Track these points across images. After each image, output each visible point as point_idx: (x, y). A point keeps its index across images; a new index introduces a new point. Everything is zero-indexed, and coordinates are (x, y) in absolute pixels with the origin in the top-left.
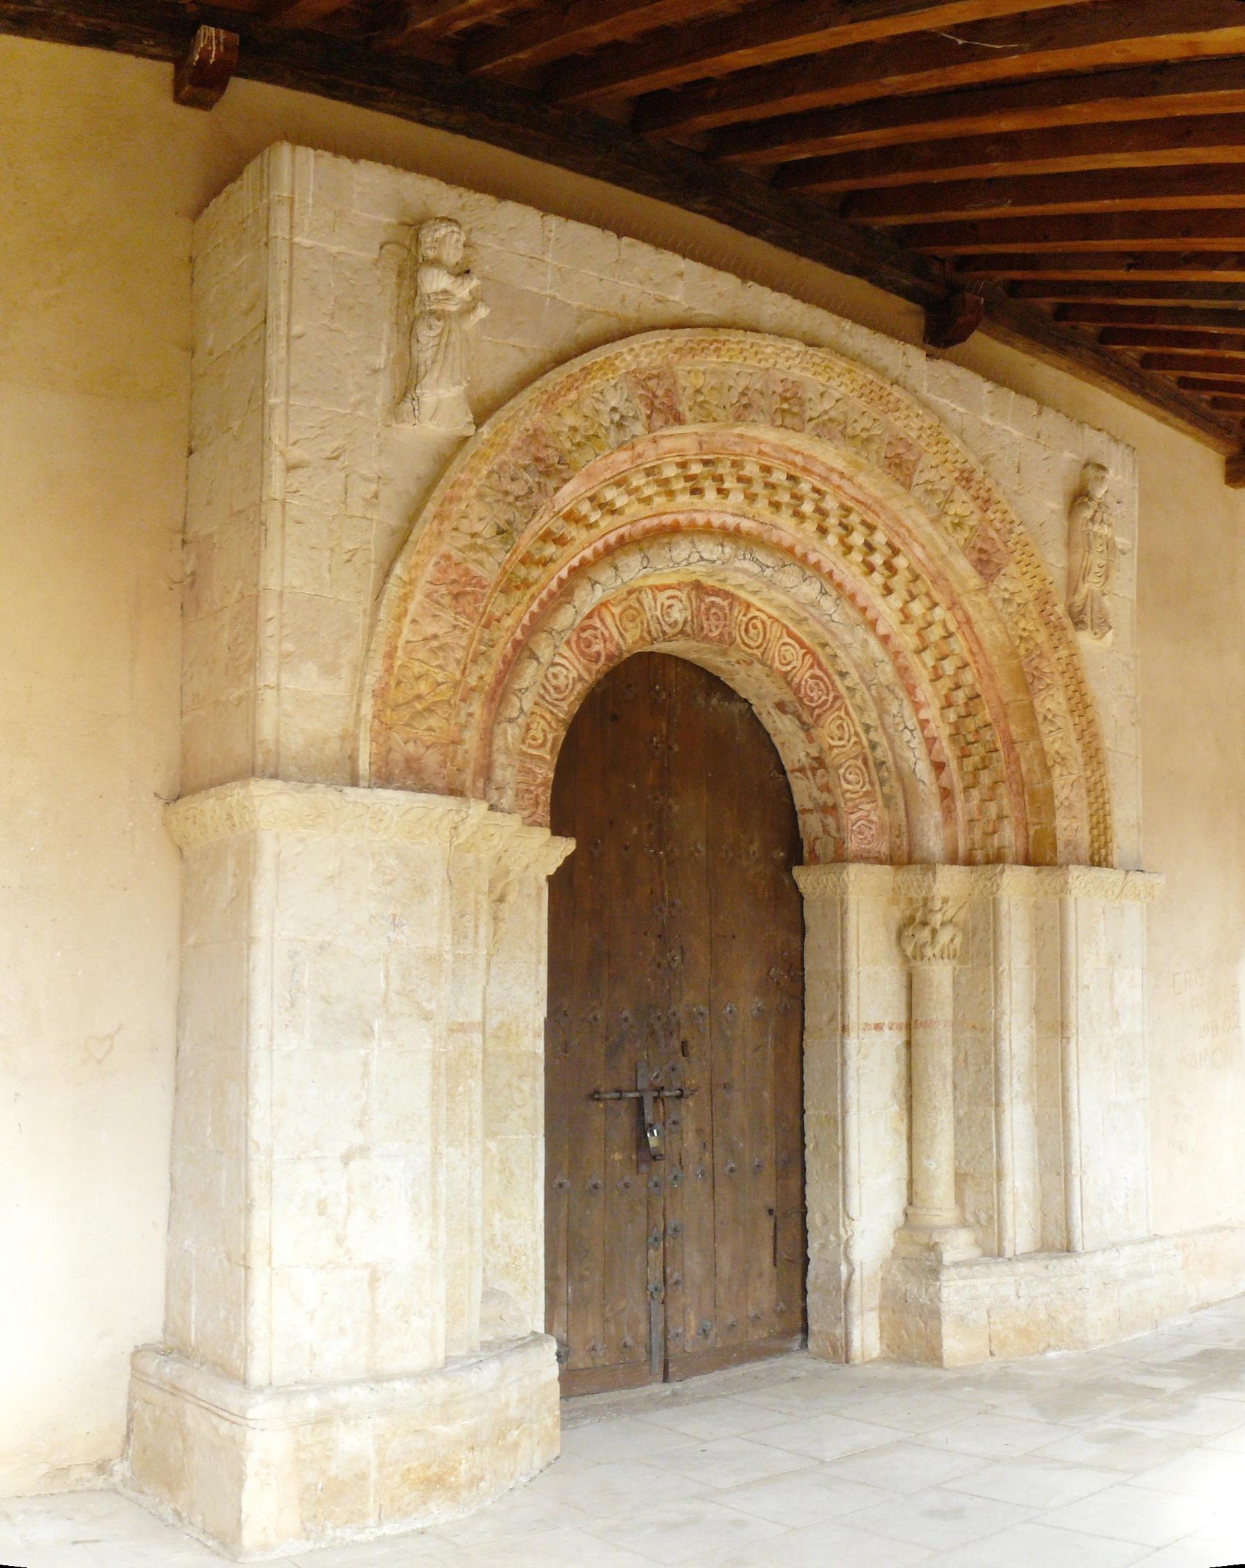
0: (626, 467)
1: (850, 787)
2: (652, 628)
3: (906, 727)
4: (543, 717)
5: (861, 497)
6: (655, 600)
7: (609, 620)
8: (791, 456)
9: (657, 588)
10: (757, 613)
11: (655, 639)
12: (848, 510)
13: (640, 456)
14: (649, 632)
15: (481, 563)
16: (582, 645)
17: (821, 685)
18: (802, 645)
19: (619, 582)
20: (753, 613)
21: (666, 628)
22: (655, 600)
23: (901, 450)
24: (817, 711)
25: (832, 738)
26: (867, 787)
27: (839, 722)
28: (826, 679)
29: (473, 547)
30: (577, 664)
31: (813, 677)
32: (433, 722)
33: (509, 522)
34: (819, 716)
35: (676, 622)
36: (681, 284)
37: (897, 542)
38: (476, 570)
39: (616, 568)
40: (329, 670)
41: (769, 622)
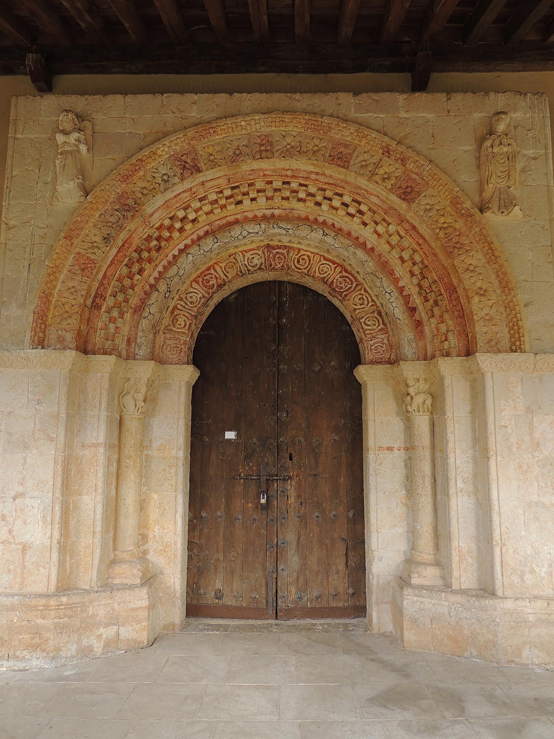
1: (369, 328)
2: (242, 270)
3: (386, 292)
4: (184, 315)
6: (244, 256)
7: (218, 269)
8: (284, 173)
9: (245, 251)
11: (244, 274)
12: (324, 190)
13: (194, 193)
14: (241, 272)
15: (95, 254)
16: (205, 282)
17: (347, 280)
18: (334, 263)
19: (202, 252)
20: (302, 252)
22: (244, 256)
23: (342, 149)
24: (344, 293)
25: (356, 305)
26: (382, 326)
28: (350, 276)
29: (93, 247)
30: (202, 291)
32: (70, 321)
35: (256, 265)
36: (195, 107)
37: (359, 199)
38: (93, 257)
39: (199, 246)
40: (22, 306)
41: (312, 256)
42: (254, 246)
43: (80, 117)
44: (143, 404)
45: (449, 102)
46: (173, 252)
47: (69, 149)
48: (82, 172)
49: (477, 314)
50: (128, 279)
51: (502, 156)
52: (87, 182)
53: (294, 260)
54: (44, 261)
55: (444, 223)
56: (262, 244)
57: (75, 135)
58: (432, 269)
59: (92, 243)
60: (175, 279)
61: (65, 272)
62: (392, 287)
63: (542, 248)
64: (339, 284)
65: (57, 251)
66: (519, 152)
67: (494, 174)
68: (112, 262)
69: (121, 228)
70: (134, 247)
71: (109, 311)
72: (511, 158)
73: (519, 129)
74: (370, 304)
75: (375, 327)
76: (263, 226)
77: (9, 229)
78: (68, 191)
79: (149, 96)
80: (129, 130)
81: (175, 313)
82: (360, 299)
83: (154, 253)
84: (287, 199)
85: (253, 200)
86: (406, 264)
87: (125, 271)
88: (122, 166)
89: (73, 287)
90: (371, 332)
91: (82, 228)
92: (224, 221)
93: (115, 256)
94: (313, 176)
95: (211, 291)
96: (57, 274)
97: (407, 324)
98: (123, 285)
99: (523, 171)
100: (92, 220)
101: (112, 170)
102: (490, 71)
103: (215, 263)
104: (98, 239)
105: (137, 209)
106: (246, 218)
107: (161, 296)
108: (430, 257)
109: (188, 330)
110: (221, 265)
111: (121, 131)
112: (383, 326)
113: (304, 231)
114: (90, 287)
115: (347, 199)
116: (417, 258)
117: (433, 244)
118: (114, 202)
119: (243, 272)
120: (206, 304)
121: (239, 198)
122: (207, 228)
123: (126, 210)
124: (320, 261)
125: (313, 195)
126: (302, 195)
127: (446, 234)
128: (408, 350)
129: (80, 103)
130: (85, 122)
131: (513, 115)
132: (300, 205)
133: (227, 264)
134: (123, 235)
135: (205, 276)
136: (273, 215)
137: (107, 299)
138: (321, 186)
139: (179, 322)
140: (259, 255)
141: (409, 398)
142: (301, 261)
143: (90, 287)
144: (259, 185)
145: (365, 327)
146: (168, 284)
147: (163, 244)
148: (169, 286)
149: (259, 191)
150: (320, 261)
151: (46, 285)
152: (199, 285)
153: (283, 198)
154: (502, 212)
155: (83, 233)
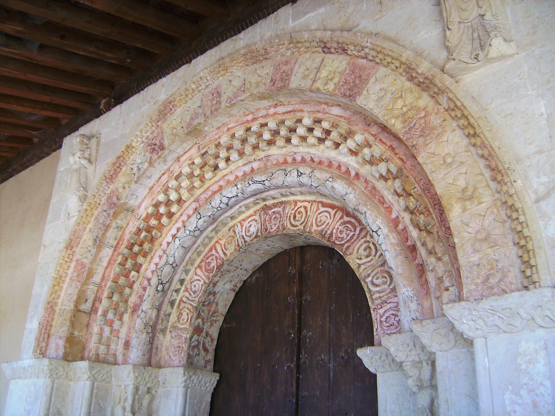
1: (378, 289)
4: (188, 308)
6: (242, 226)
11: (241, 248)
17: (349, 226)
19: (188, 232)
20: (299, 204)
22: (242, 226)
24: (346, 245)
27: (365, 245)
30: (203, 277)
31: (345, 223)
34: (348, 247)
37: (320, 116)
41: (308, 205)
42: (251, 211)
49: (459, 233)
58: (413, 180)
60: (165, 269)
61: (68, 280)
64: (339, 235)
70: (125, 243)
71: (105, 314)
75: (386, 286)
76: (239, 186)
81: (181, 307)
82: (365, 249)
90: (381, 295)
92: (210, 193)
94: (272, 111)
95: (211, 275)
96: (61, 285)
97: (401, 275)
100: (90, 226)
108: (408, 163)
119: (241, 245)
124: (318, 209)
137: (103, 301)
146: (158, 276)
148: (159, 277)
150: (318, 209)
151: (51, 296)
152: (202, 271)
155: (82, 240)
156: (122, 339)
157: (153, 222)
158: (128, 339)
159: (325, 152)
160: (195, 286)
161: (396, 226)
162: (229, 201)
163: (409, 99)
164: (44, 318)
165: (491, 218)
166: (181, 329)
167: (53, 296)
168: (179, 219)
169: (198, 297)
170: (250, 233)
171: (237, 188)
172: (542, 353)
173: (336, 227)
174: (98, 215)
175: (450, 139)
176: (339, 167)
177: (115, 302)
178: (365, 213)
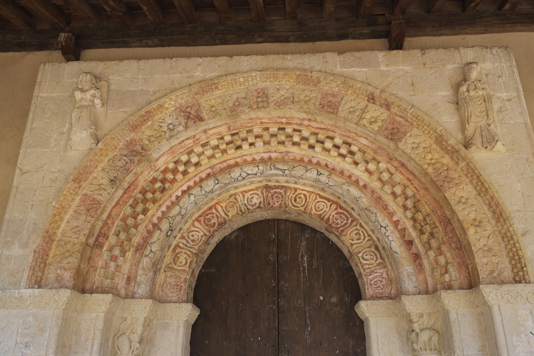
0: (191, 145)
1: (367, 262)
3: (381, 226)
4: (186, 253)
5: (323, 126)
6: (244, 196)
7: (219, 209)
8: (279, 120)
9: (245, 192)
10: (301, 192)
11: (244, 213)
12: (316, 134)
13: (197, 140)
14: (241, 211)
15: (101, 195)
16: (206, 221)
17: (343, 216)
18: (329, 200)
20: (299, 192)
21: (250, 207)
22: (244, 196)
23: (331, 99)
24: (341, 229)
25: (353, 240)
26: (380, 260)
27: (356, 232)
28: (345, 213)
29: (99, 190)
30: (203, 230)
31: (338, 213)
32: (70, 260)
33: (115, 177)
34: (342, 231)
35: (256, 204)
36: (199, 68)
37: (349, 140)
38: (99, 198)
39: (201, 187)
40: (25, 246)
41: (308, 194)
42: (253, 186)
43: (97, 78)
44: (138, 345)
45: (424, 57)
46: (176, 193)
47: (86, 104)
48: (95, 123)
49: (474, 245)
50: (132, 219)
51: (478, 99)
52: (99, 132)
53: (291, 199)
54: (52, 202)
55: (431, 159)
56: (261, 185)
57: (92, 92)
58: (424, 203)
59: (99, 185)
60: (177, 218)
61: (71, 212)
62: (387, 221)
63: (529, 179)
64: (335, 220)
65: (64, 193)
66: (493, 95)
67: (473, 114)
68: (117, 203)
69: (128, 171)
70: (139, 188)
71: (111, 249)
72: (487, 100)
73: (490, 76)
74: (367, 239)
75: (373, 261)
76: (261, 168)
77: (23, 174)
78: (81, 139)
79: (159, 61)
80: (140, 88)
81: (177, 251)
82: (356, 234)
83: (158, 194)
84: (283, 143)
85: (251, 144)
86: (399, 199)
87: (129, 210)
88: (132, 117)
89: (77, 227)
90: (370, 266)
91: (91, 173)
92: (225, 165)
93: (121, 197)
94: (306, 123)
95: (212, 229)
96: (62, 215)
97: (405, 258)
98: (126, 224)
99: (500, 111)
101: (123, 121)
102: (456, 34)
103: (216, 203)
104: (105, 181)
105: (144, 154)
106: (245, 161)
107: (163, 234)
108: (421, 191)
109: (189, 267)
110: (222, 204)
111: (133, 89)
112: (381, 261)
113: (299, 171)
114: (93, 226)
115: (338, 141)
116: (409, 192)
117: (423, 179)
118: (123, 149)
119: (243, 211)
120: (207, 243)
121: (239, 143)
122: (208, 171)
123: (133, 156)
124: (316, 199)
125: (306, 139)
126: (296, 139)
127: (434, 169)
128: (409, 285)
129: (99, 67)
130: (102, 82)
131: (483, 66)
132: (294, 150)
133: (228, 204)
134: (129, 178)
135: (207, 215)
136: (270, 158)
137: (110, 238)
138: (314, 130)
139: (180, 260)
140: (258, 195)
141: (414, 335)
142: (298, 200)
143: (93, 226)
144: (257, 130)
145: (364, 262)
146: (170, 223)
147: (167, 185)
148: (171, 224)
149: (257, 137)
150: (316, 199)
151: (50, 225)
152: (201, 224)
153: (279, 143)
154: (486, 148)
155: (91, 176)
156: (124, 274)
157: (170, 176)
158: (129, 275)
159: (346, 165)
160: (193, 236)
161: (396, 227)
162: (247, 176)
163: (436, 156)
164: (40, 247)
165: (492, 240)
166: (179, 270)
167: (53, 225)
168: (192, 178)
169: (198, 246)
170: (253, 203)
171: (259, 169)
172: (530, 316)
173: (332, 215)
174: (114, 157)
175: (465, 188)
176: (350, 177)
177: (120, 241)
178: (376, 213)
